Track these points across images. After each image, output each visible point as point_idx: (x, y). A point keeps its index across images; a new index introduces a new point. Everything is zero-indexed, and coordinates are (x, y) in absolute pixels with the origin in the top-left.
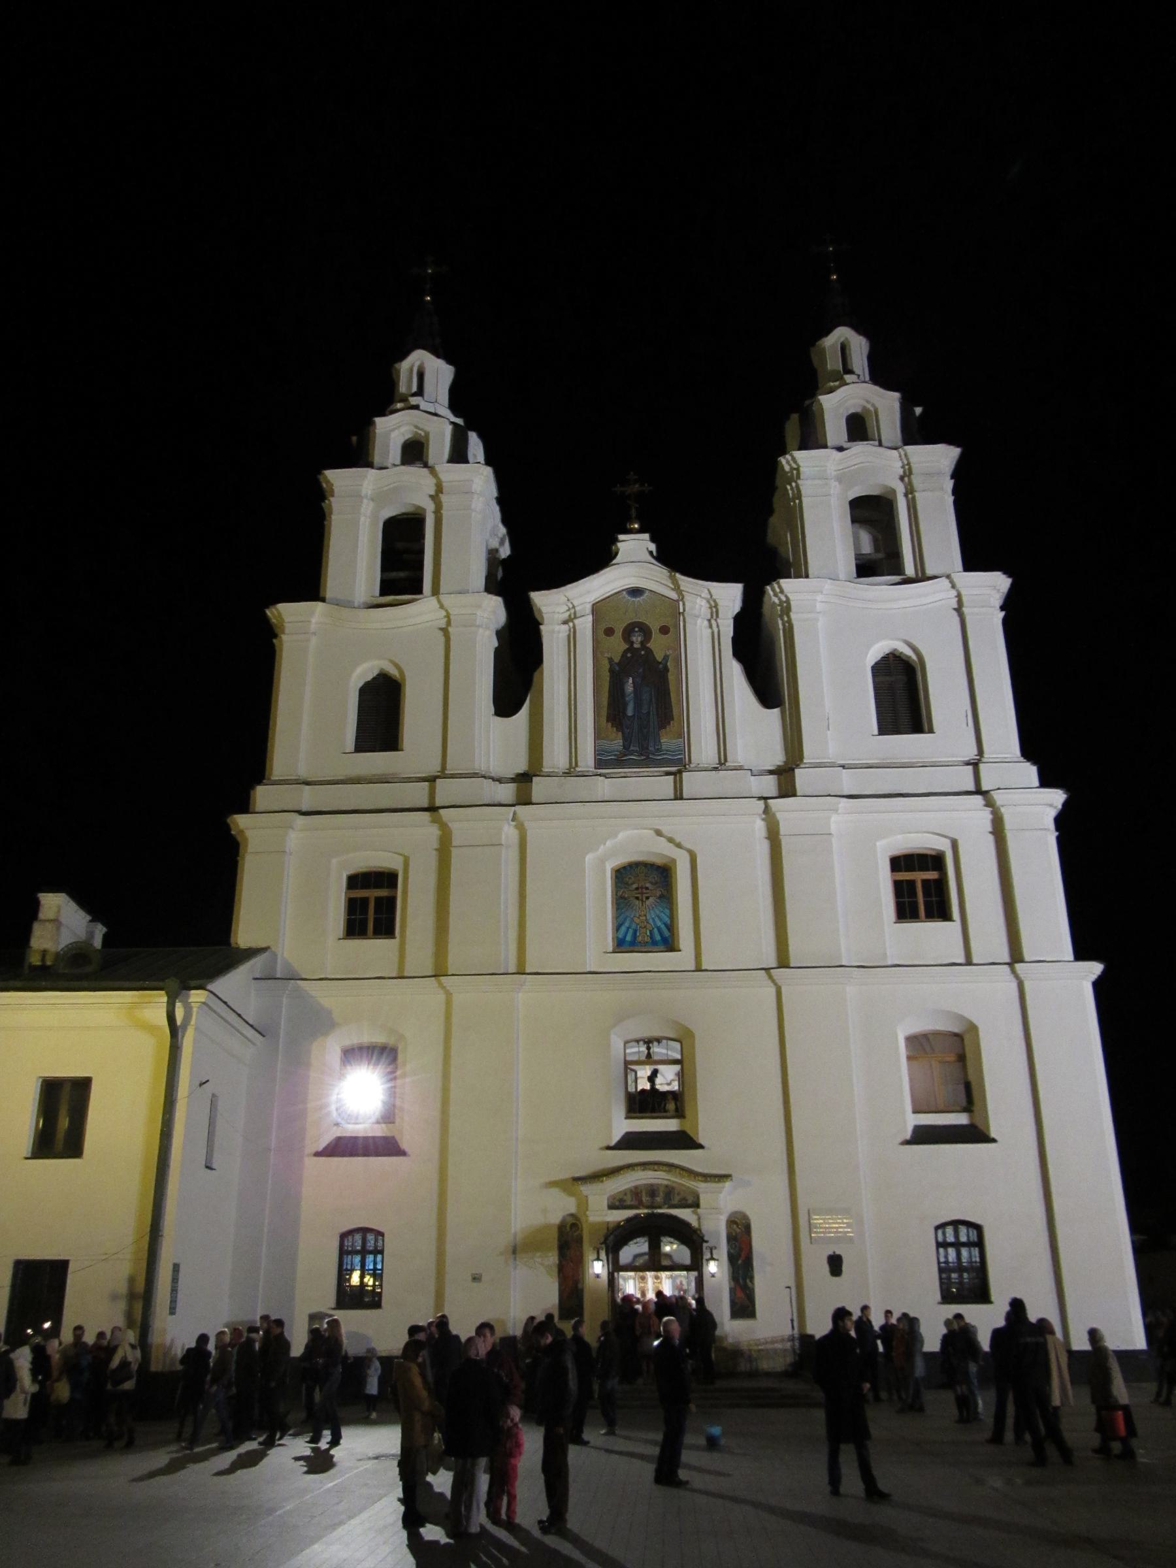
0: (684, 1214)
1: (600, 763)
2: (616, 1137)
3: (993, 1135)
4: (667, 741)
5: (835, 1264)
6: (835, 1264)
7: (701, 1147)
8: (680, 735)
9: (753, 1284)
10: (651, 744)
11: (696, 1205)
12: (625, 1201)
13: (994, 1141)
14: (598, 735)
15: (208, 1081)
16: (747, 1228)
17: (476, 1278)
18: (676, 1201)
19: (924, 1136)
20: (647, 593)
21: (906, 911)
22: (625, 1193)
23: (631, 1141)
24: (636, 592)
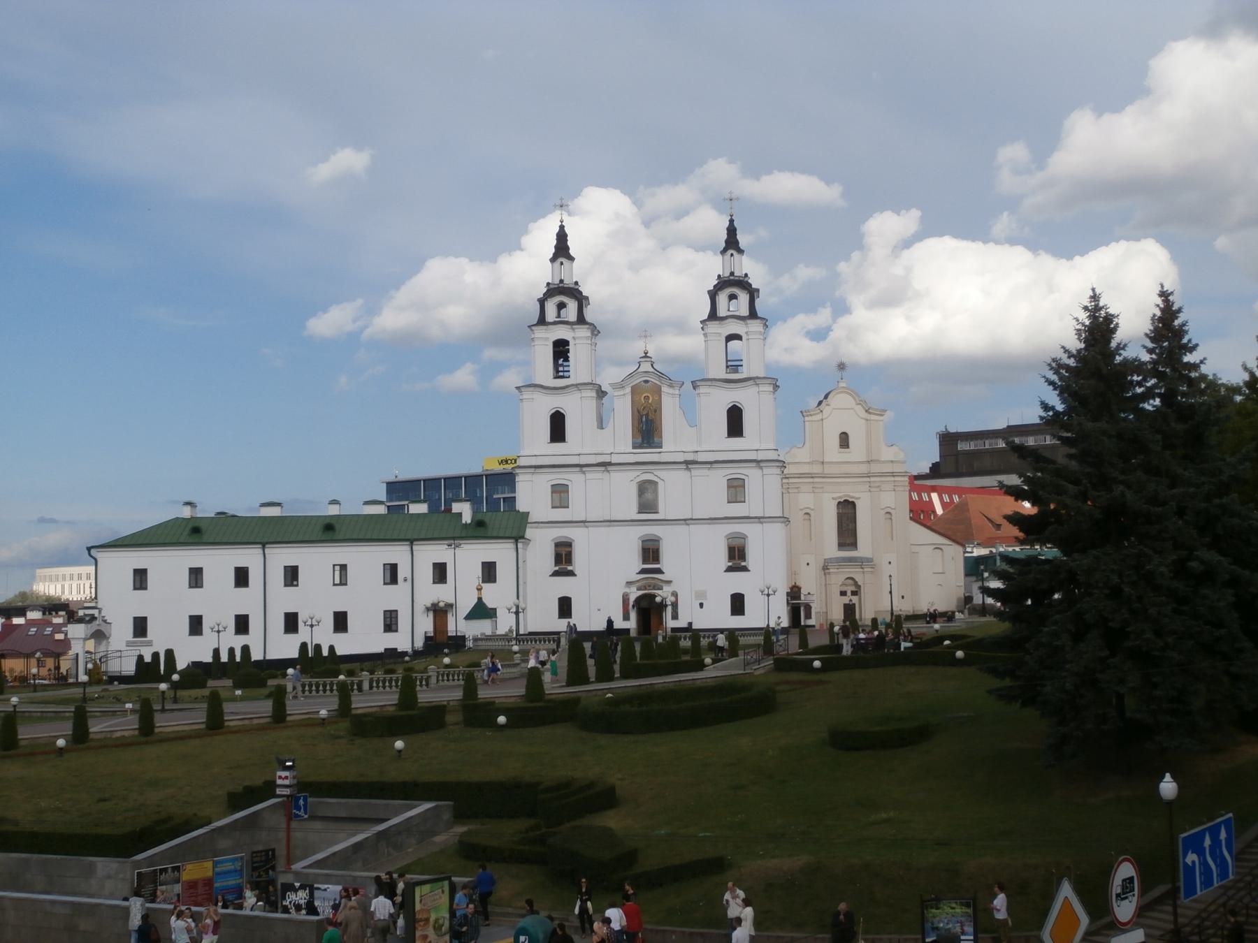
1: (634, 447)
3: (749, 569)
4: (656, 440)
5: (701, 605)
6: (701, 605)
8: (661, 437)
11: (662, 589)
13: (749, 571)
14: (633, 437)
17: (599, 610)
18: (656, 588)
23: (643, 571)
24: (646, 382)
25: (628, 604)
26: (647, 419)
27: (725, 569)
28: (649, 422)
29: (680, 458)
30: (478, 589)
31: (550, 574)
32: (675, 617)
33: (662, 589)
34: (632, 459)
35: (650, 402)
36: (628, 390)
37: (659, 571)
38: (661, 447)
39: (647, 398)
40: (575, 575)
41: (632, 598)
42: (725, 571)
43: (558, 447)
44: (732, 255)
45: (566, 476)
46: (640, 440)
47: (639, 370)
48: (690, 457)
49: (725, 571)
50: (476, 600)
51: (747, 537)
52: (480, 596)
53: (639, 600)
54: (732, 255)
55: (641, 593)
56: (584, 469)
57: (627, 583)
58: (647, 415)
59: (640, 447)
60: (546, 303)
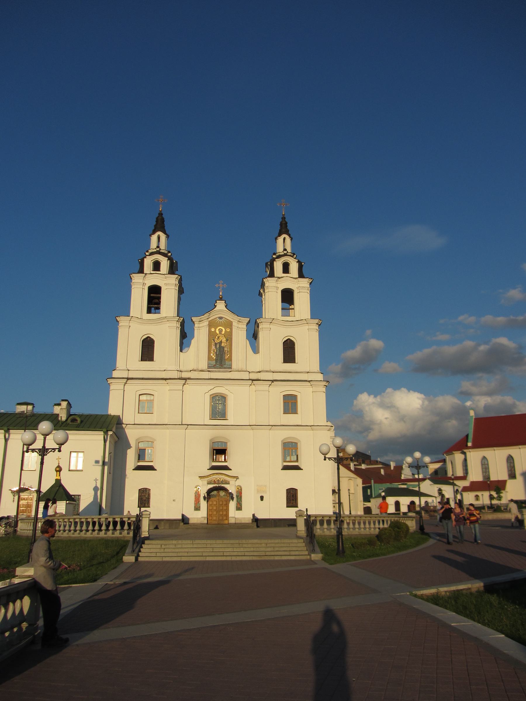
0: (226, 486)
1: (209, 367)
2: (210, 467)
5: (262, 498)
6: (262, 498)
7: (231, 470)
8: (231, 360)
9: (242, 502)
10: (223, 363)
12: (211, 482)
13: (302, 469)
15: (111, 453)
16: (241, 489)
17: (174, 500)
19: (285, 468)
20: (224, 319)
21: (286, 412)
22: (212, 480)
23: (213, 468)
24: (221, 318)
25: (199, 495)
26: (220, 346)
27: (281, 468)
28: (222, 349)
29: (246, 376)
30: (57, 471)
31: (134, 468)
32: (239, 508)
33: (229, 484)
34: (206, 375)
35: (223, 333)
36: (206, 323)
37: (226, 468)
38: (231, 368)
39: (221, 331)
40: (156, 470)
41: (203, 492)
42: (282, 470)
43: (147, 364)
44: (284, 239)
45: (150, 387)
46: (214, 363)
47: (215, 309)
48: (253, 376)
49: (282, 470)
50: (54, 482)
51: (300, 441)
52: (58, 478)
53: (209, 491)
54: (284, 239)
55: (211, 486)
56: (168, 381)
57: (199, 477)
58: (221, 342)
59: (214, 367)
60: (145, 259)
